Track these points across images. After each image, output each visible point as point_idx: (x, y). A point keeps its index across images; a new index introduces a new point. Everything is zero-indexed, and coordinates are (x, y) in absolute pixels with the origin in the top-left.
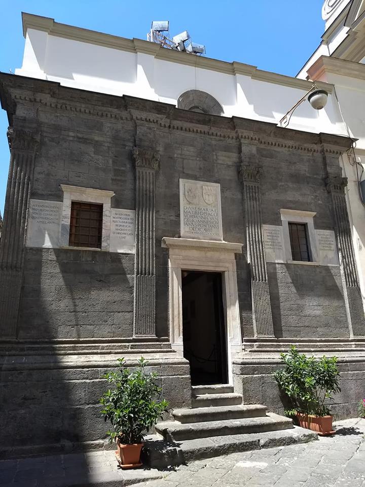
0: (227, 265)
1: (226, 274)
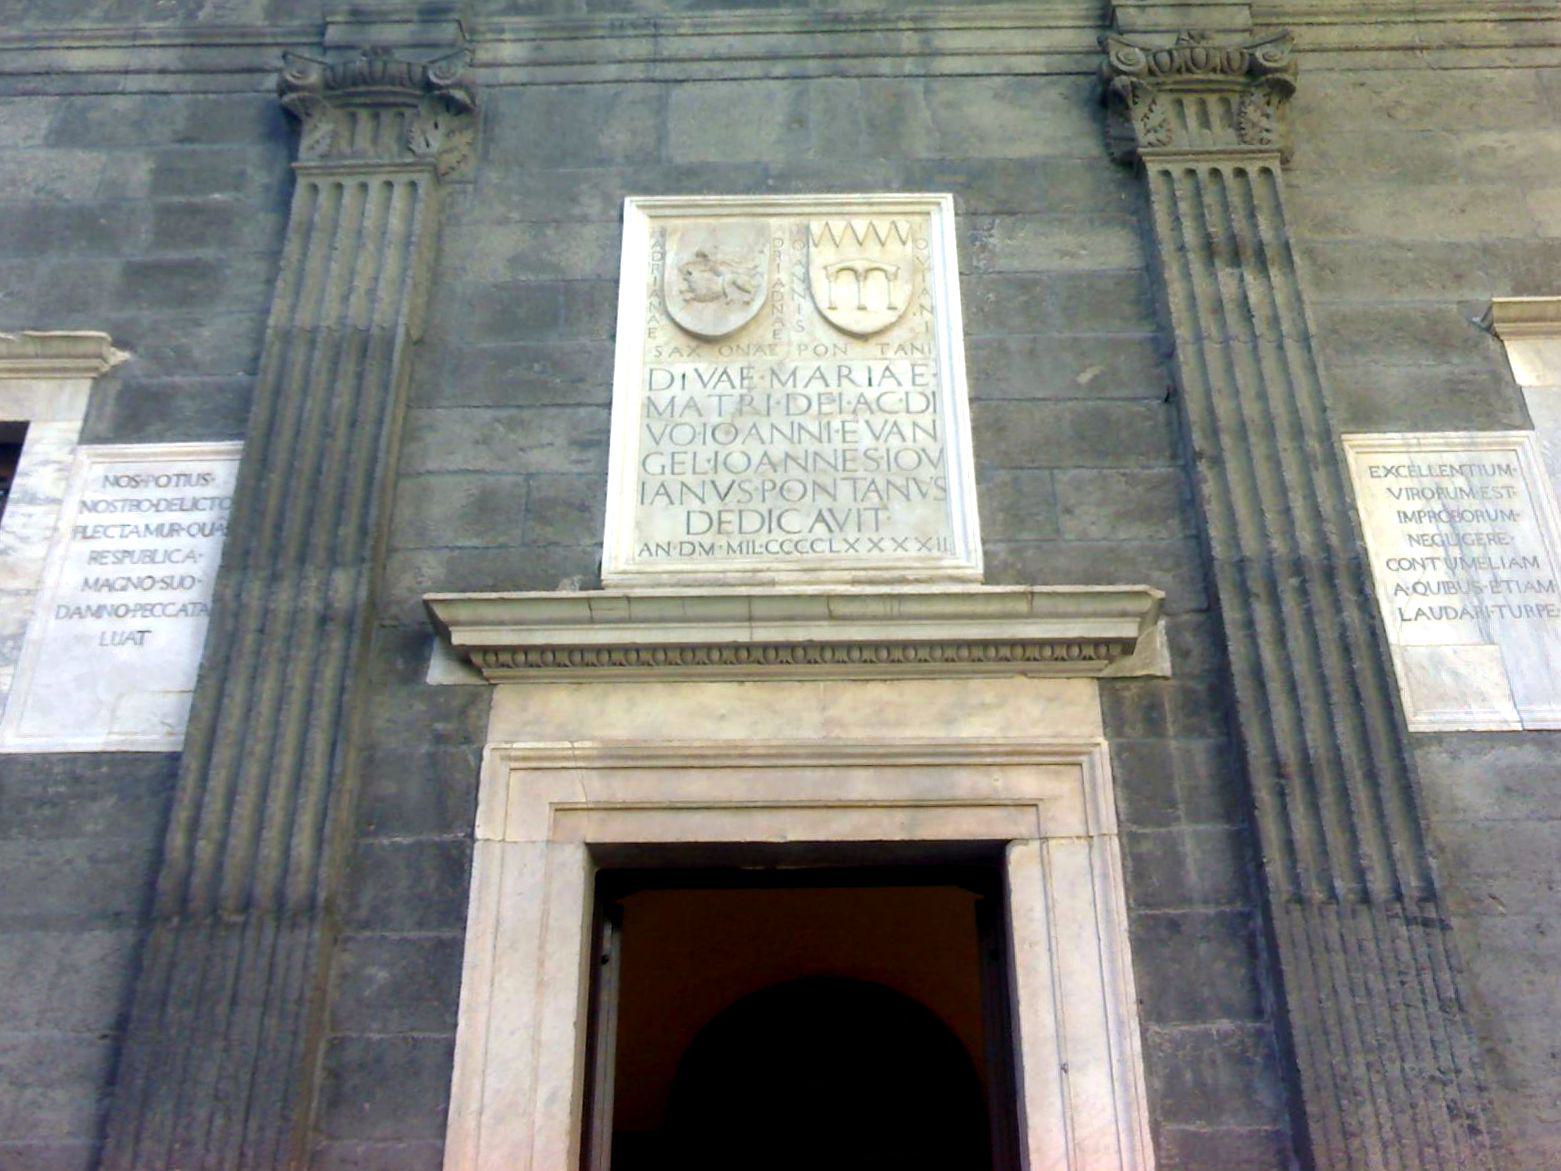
0: (1026, 783)
1: (1015, 855)
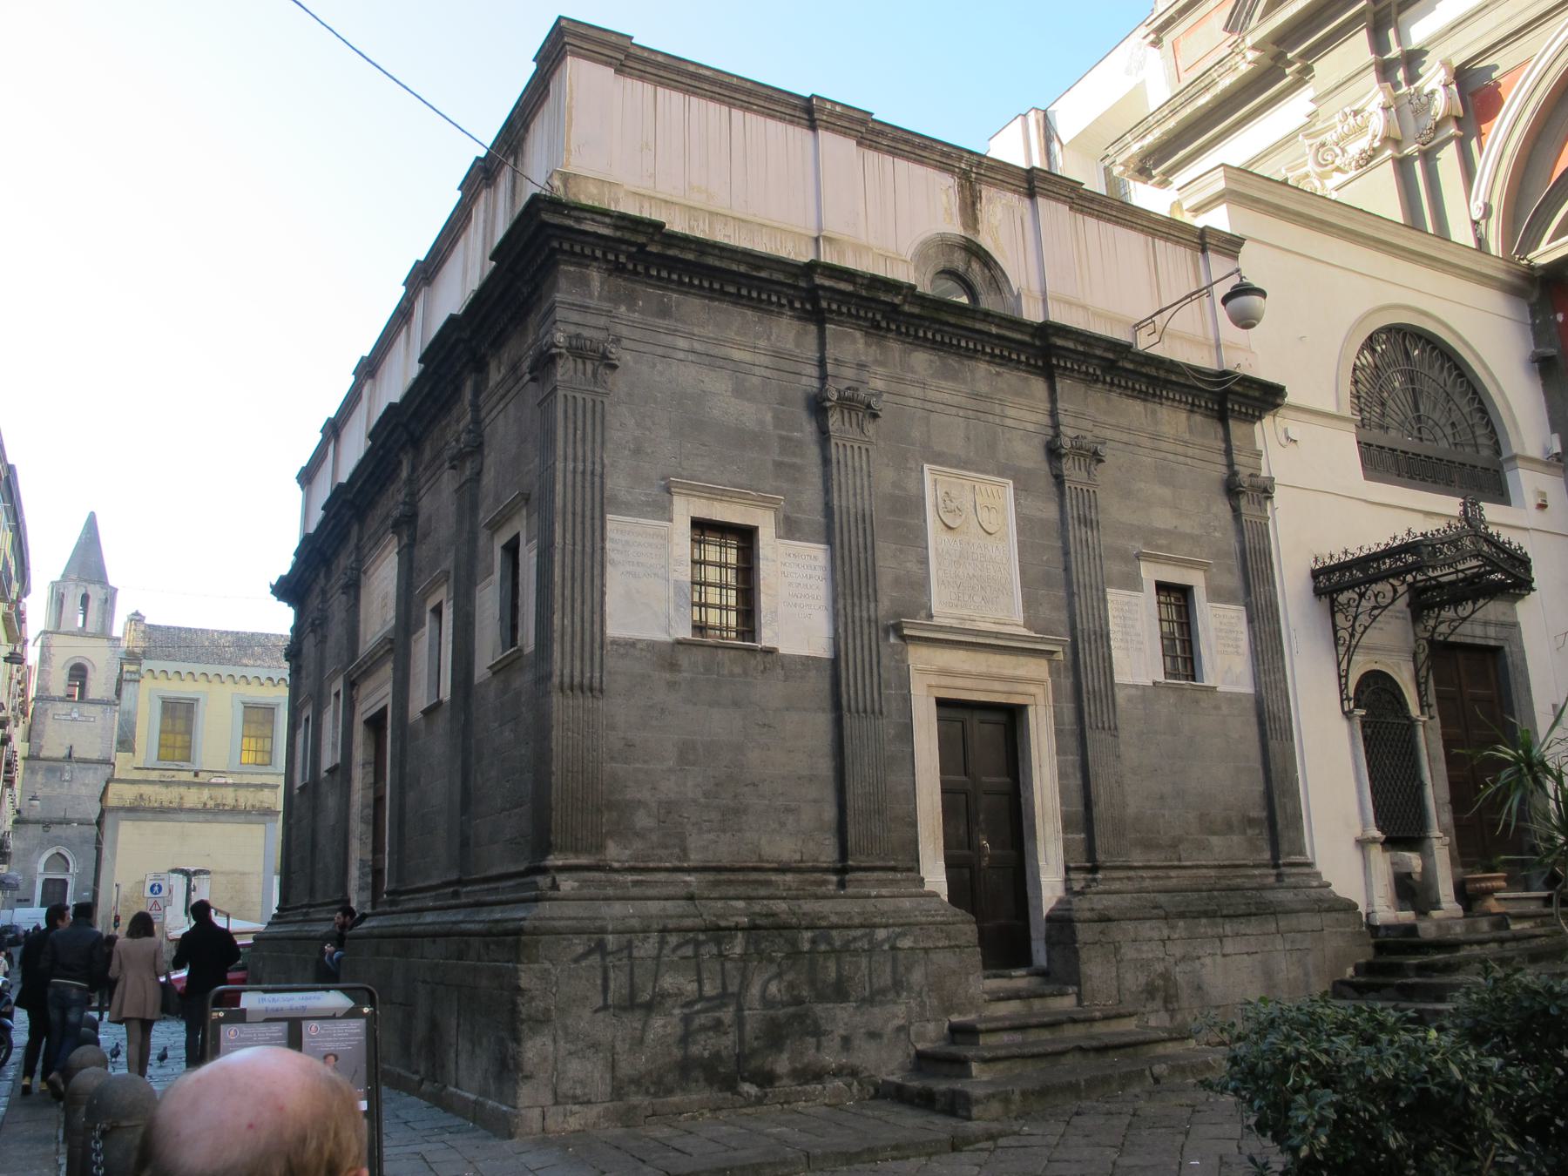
0: (1032, 689)
1: (1031, 711)
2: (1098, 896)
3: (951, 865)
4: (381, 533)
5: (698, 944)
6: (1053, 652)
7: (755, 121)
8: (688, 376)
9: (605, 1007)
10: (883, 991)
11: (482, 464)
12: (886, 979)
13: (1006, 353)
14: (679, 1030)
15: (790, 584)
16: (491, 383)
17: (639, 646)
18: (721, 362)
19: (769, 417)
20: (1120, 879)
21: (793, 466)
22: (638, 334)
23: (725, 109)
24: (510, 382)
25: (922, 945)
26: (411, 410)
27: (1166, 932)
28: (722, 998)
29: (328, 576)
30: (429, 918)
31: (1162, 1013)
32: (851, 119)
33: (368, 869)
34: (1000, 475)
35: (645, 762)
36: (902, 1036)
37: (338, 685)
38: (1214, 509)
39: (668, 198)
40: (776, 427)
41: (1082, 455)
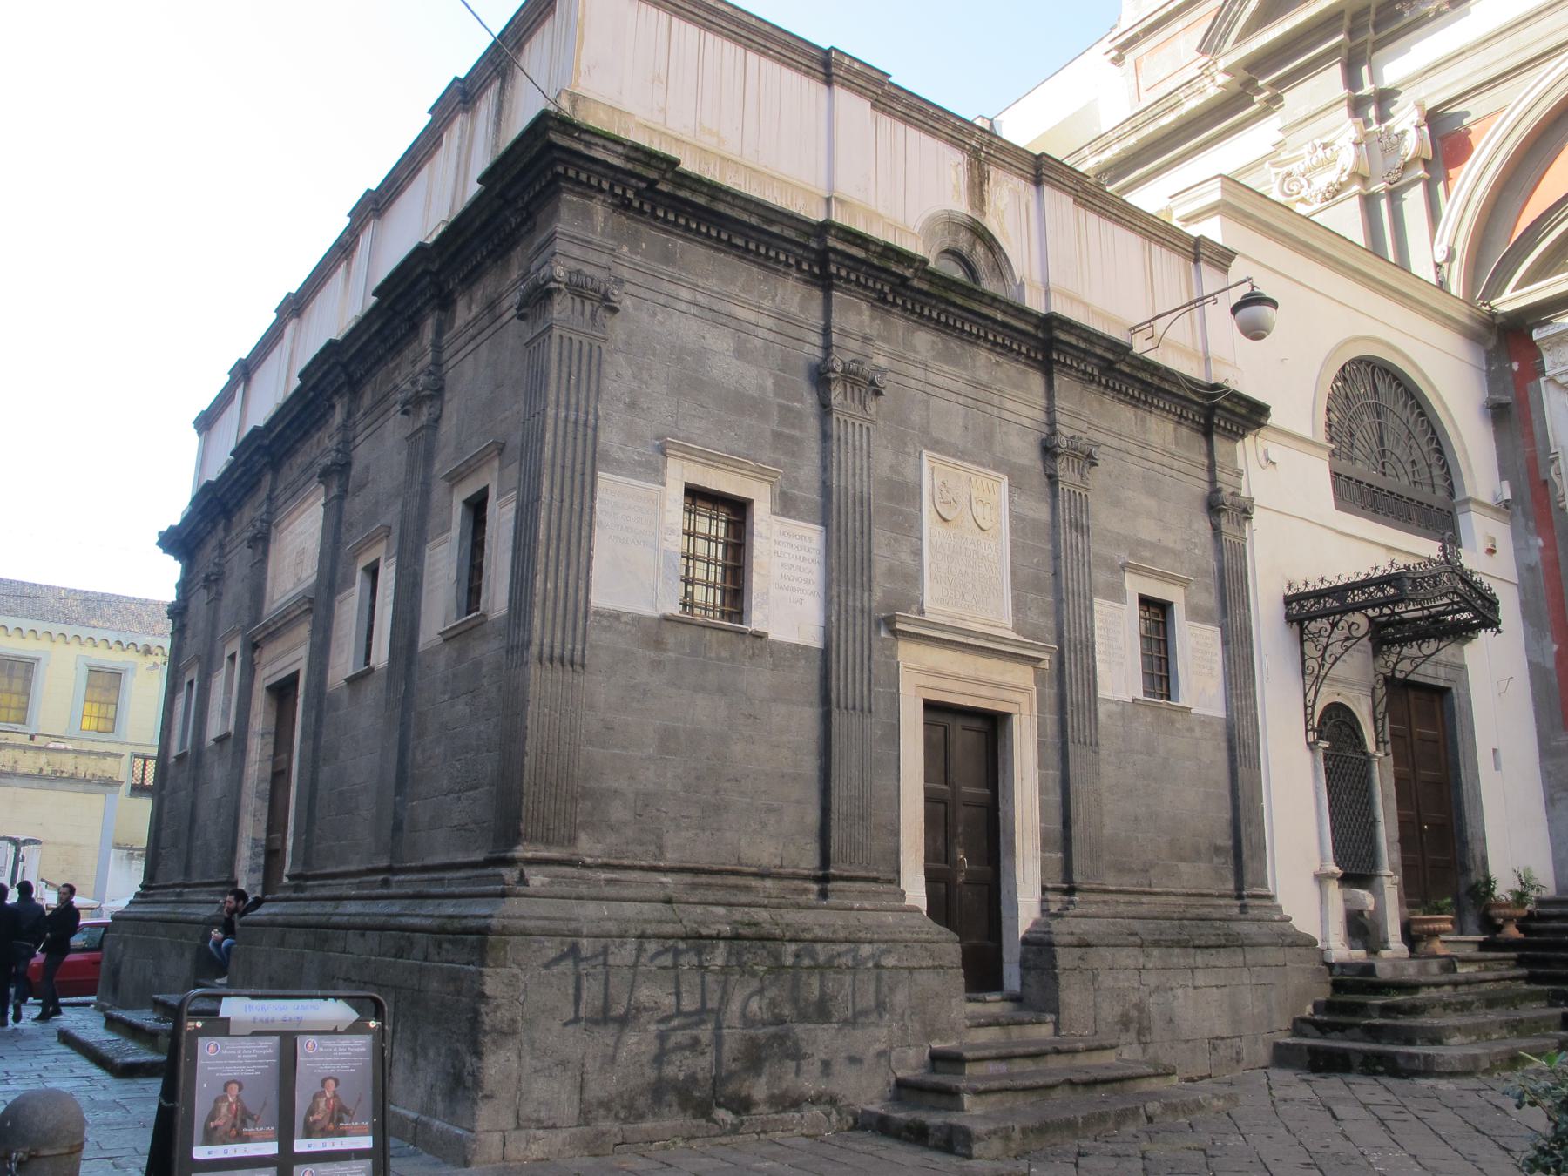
0: (1018, 697)
1: (1015, 719)
2: (1075, 920)
3: (932, 878)
4: (301, 483)
5: (677, 953)
6: (1040, 660)
7: (771, 68)
8: (688, 329)
9: (576, 1020)
10: (865, 1013)
11: (441, 410)
12: (869, 1000)
13: (1007, 342)
14: (654, 1049)
15: (783, 565)
16: (459, 322)
17: (624, 619)
18: (724, 320)
19: (769, 383)
20: (1096, 902)
21: (791, 438)
22: (640, 279)
23: (740, 50)
24: (485, 322)
25: (906, 964)
26: (353, 350)
27: (1141, 961)
28: (701, 1015)
29: (227, 529)
30: (352, 907)
31: (1135, 1046)
32: (869, 79)
33: (260, 850)
34: (996, 468)
35: (624, 748)
36: (883, 1061)
37: (235, 646)
38: (1196, 526)
39: (679, 137)
40: (776, 395)
41: (1076, 457)
